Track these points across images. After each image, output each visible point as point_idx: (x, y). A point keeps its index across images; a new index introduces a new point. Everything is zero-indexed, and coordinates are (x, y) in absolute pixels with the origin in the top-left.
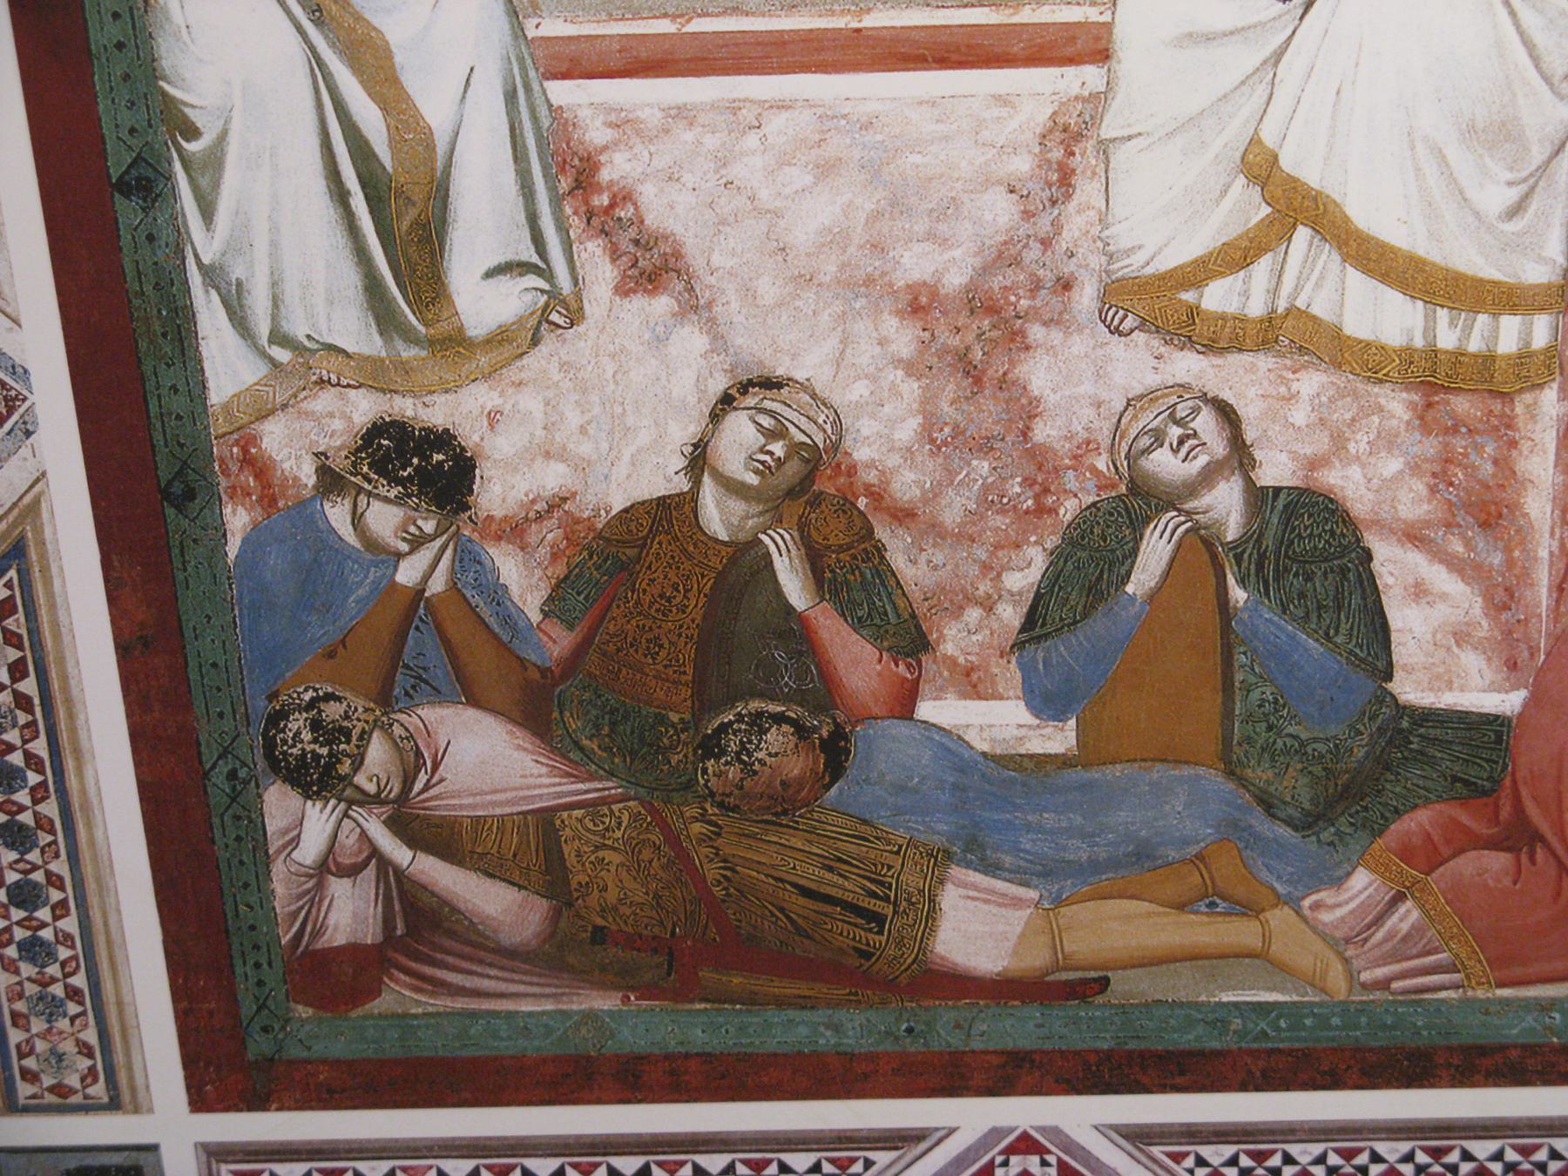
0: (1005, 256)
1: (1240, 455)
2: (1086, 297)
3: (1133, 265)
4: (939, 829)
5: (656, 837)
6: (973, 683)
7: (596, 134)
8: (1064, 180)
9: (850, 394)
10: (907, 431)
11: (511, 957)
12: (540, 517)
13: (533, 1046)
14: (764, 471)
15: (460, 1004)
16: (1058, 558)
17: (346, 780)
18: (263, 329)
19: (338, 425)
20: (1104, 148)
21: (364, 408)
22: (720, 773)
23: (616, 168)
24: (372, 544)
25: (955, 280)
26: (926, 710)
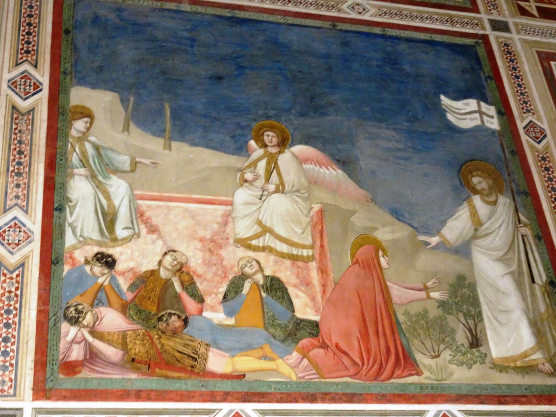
0: (216, 234)
1: (261, 269)
2: (231, 241)
3: (238, 237)
4: (208, 339)
5: (147, 338)
6: (213, 309)
7: (145, 208)
8: (226, 223)
9: (190, 254)
10: (200, 261)
11: (113, 364)
12: (128, 271)
13: (116, 387)
14: (173, 266)
15: (99, 375)
16: (229, 286)
17: (81, 322)
18: (78, 234)
19: (90, 252)
20: (233, 218)
21: (96, 249)
22: (162, 325)
23: (148, 214)
24: (94, 274)
25: (208, 237)
26: (205, 314)
